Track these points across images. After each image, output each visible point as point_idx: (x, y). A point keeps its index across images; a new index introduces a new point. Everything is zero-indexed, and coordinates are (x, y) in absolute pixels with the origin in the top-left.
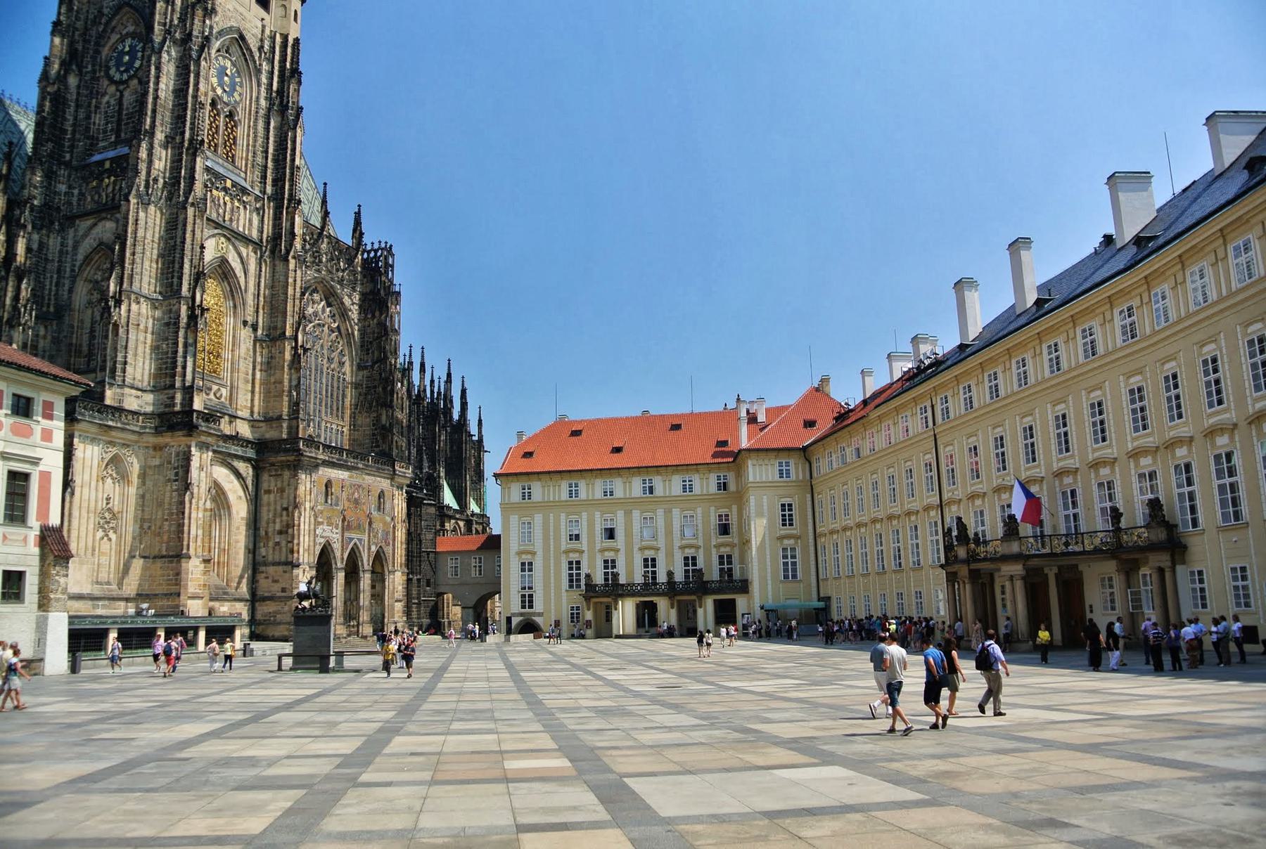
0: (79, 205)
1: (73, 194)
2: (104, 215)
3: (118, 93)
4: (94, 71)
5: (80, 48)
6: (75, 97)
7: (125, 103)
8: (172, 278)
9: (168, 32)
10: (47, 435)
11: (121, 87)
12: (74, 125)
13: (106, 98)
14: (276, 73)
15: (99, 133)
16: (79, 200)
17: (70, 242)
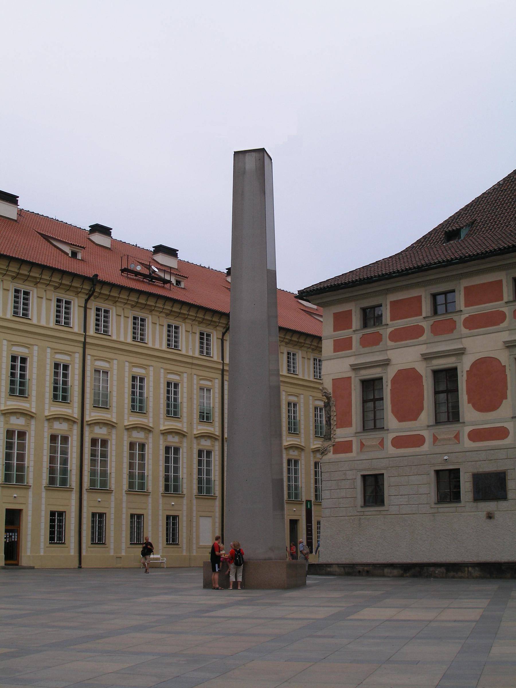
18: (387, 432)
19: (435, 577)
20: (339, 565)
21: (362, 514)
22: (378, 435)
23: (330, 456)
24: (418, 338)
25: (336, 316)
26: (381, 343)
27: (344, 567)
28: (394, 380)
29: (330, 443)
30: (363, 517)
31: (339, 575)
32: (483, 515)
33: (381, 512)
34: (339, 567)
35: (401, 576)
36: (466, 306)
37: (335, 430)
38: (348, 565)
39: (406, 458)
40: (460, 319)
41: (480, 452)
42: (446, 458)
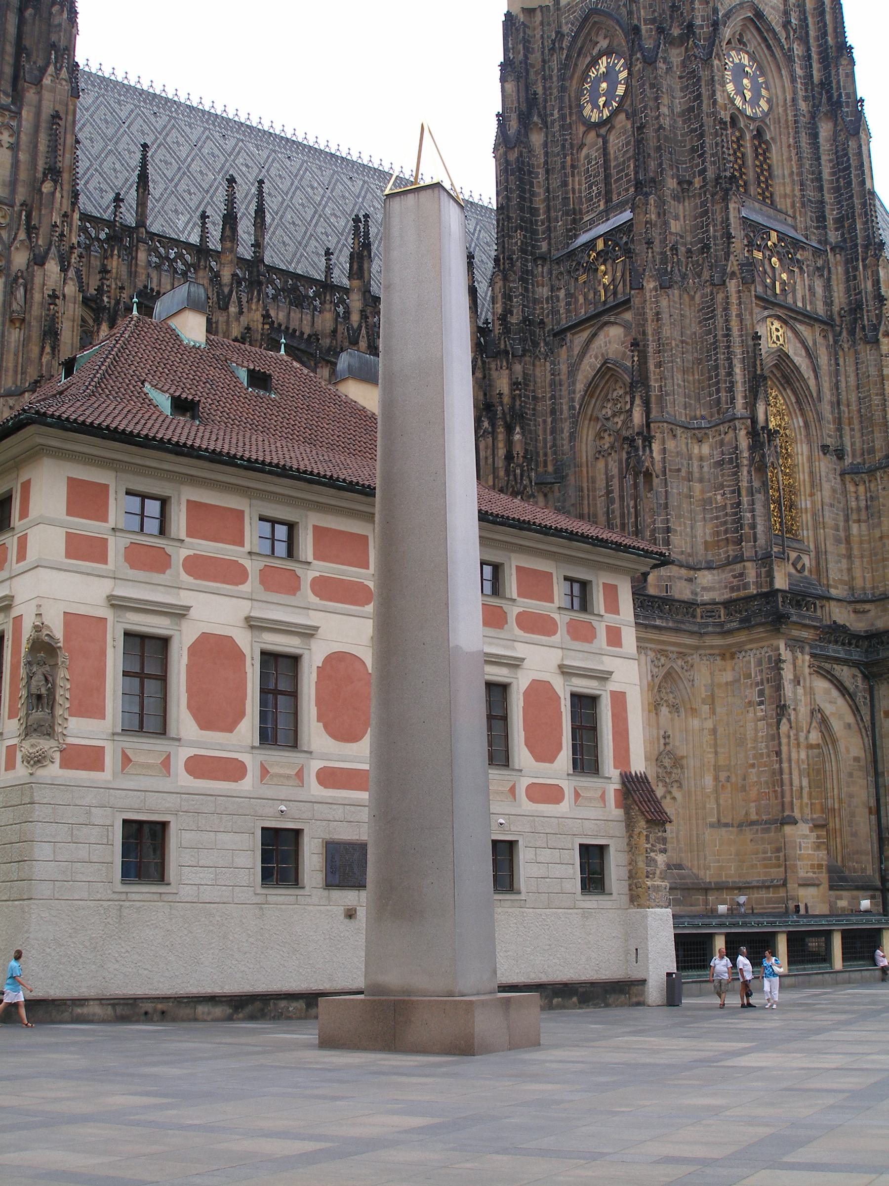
0: (568, 311)
1: (558, 297)
2: (605, 318)
3: (600, 140)
4: (563, 117)
5: (540, 90)
6: (542, 160)
7: (612, 150)
8: (718, 391)
9: (661, 30)
10: (614, 637)
11: (603, 131)
12: (547, 199)
13: (584, 151)
14: (815, 56)
15: (581, 203)
16: (568, 304)
17: (564, 368)
18: (177, 743)
19: (289, 1018)
20: (104, 1002)
21: (123, 897)
22: (158, 746)
23: (53, 771)
24: (237, 584)
25: (74, 485)
26: (168, 572)
27: (114, 1006)
28: (194, 650)
29: (53, 743)
30: (127, 904)
31: (103, 1021)
32: (340, 911)
33: (163, 896)
34: (101, 1004)
35: (230, 1018)
36: (316, 558)
37: (66, 719)
38: (122, 1002)
39: (213, 798)
40: (308, 576)
41: (335, 807)
42: (284, 808)
